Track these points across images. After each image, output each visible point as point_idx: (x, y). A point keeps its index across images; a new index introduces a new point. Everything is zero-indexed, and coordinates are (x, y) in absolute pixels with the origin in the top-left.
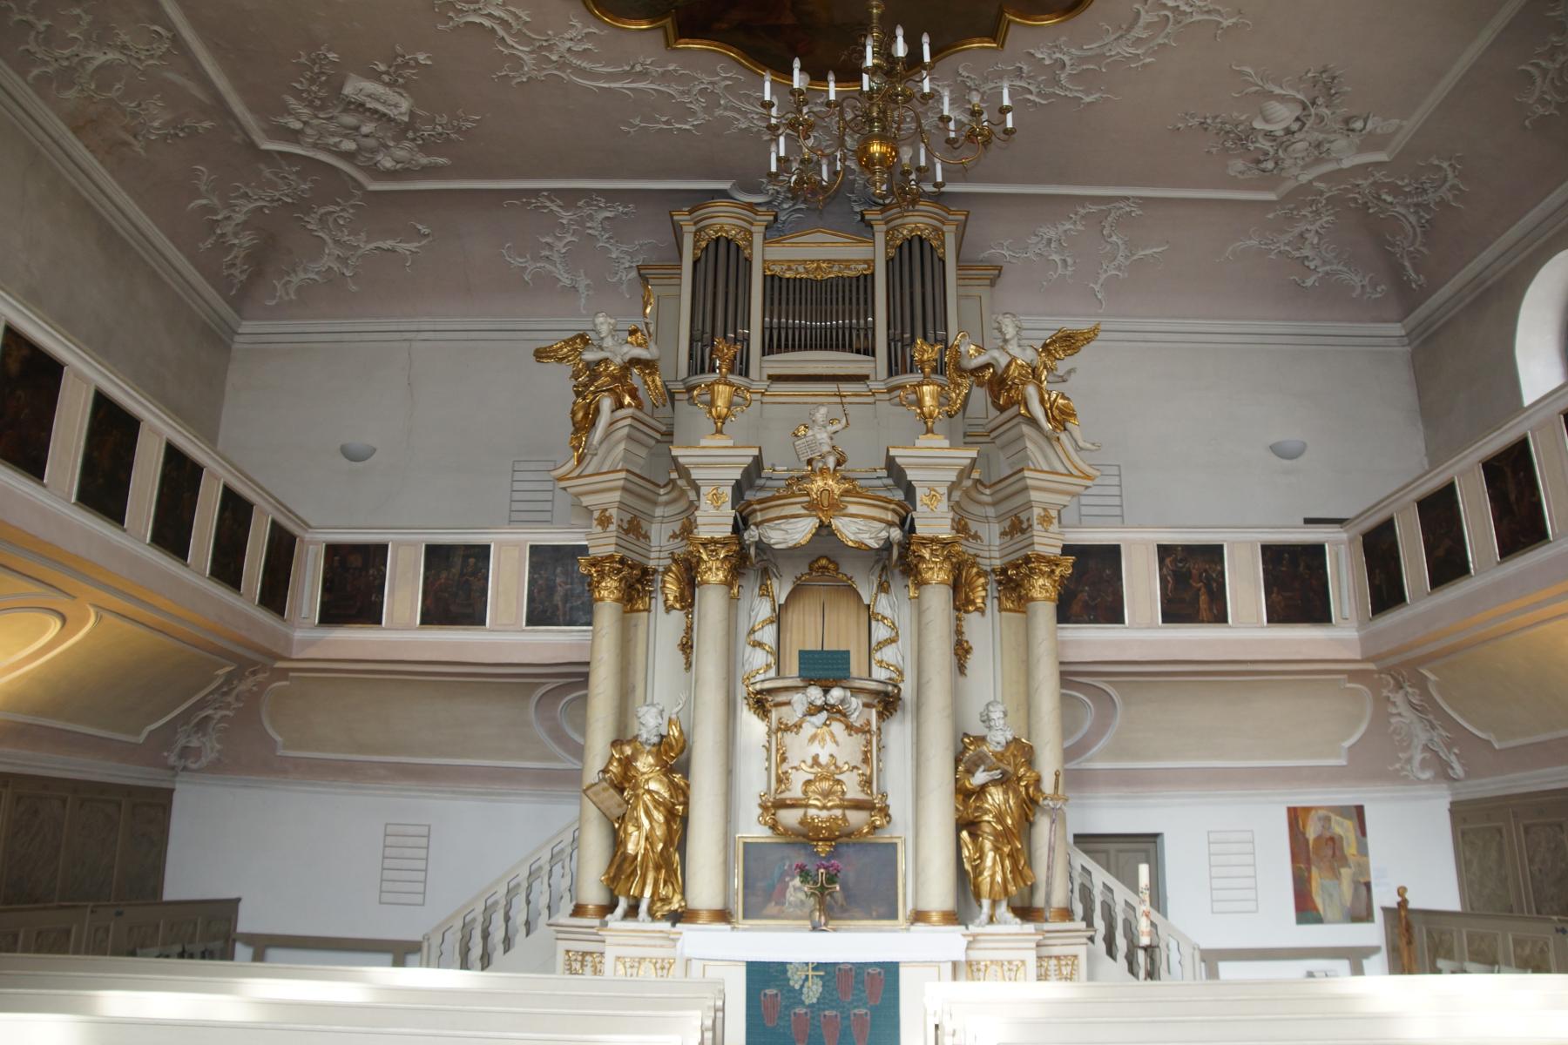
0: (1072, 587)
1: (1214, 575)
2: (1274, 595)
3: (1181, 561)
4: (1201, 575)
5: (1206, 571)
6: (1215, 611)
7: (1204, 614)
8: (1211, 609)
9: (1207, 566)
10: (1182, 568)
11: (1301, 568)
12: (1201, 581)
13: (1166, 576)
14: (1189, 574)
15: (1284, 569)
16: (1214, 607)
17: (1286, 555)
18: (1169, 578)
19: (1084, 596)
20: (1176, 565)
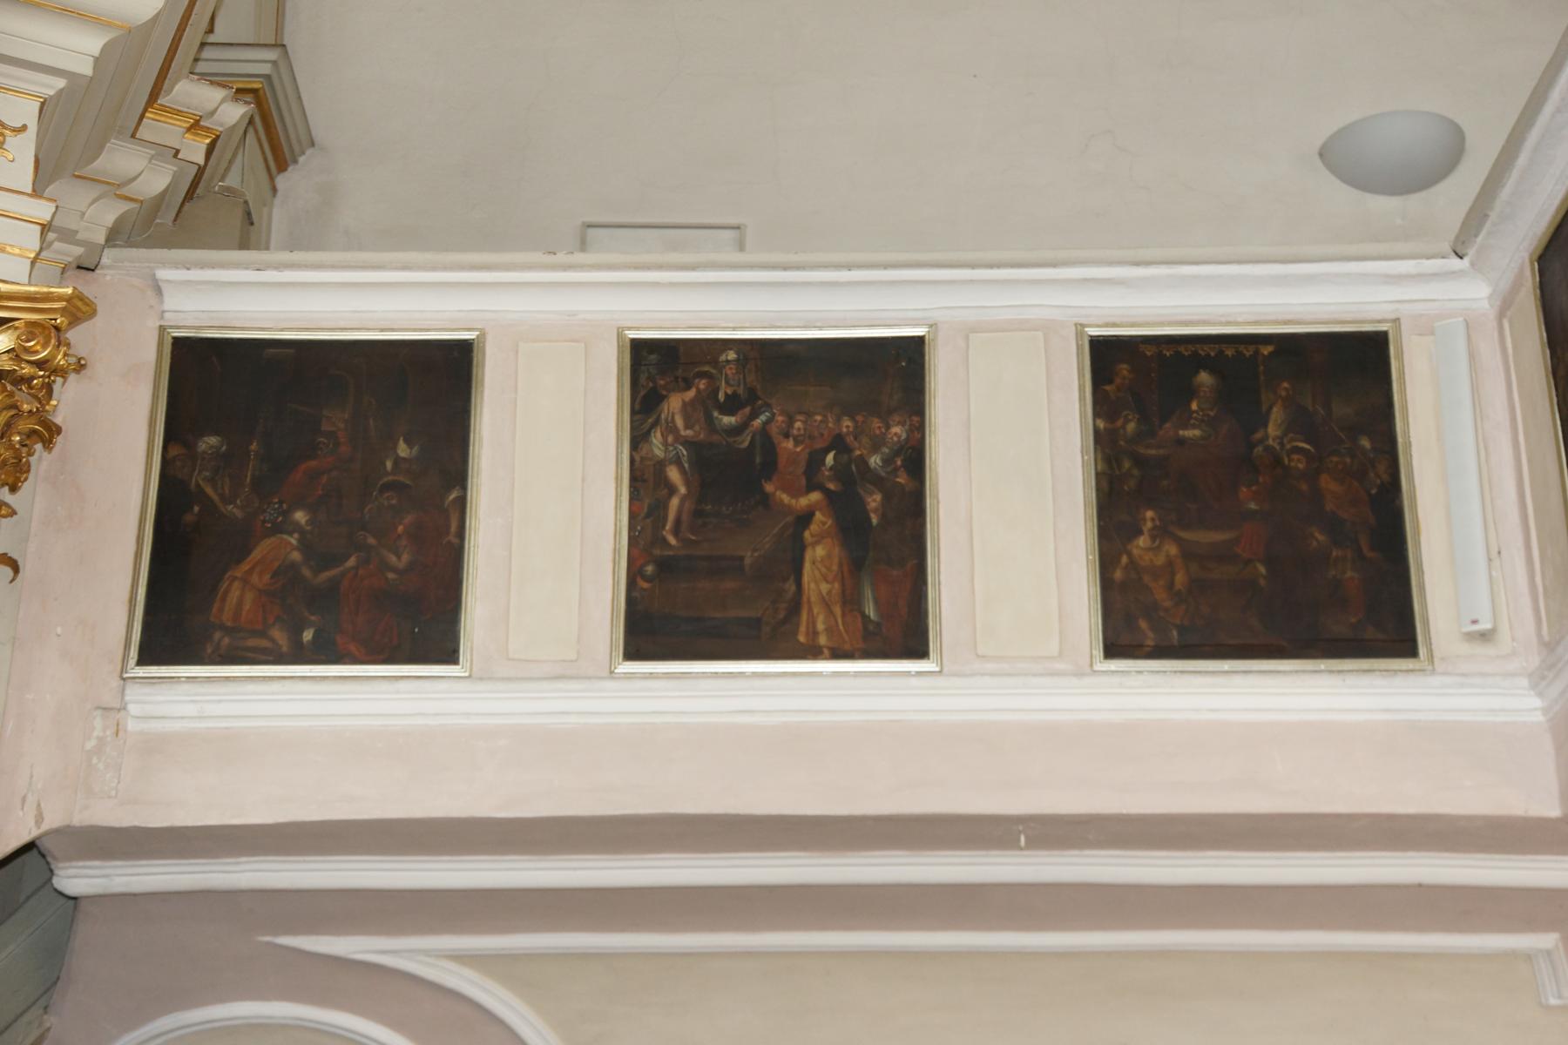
0: (234, 510)
1: (875, 461)
2: (1142, 541)
3: (731, 405)
4: (815, 461)
5: (839, 444)
6: (871, 611)
7: (818, 620)
8: (851, 601)
9: (847, 423)
10: (737, 431)
11: (1273, 430)
12: (820, 487)
13: (660, 466)
14: (765, 459)
15: (1192, 433)
16: (868, 593)
17: (1204, 378)
18: (674, 474)
19: (289, 547)
20: (710, 420)
